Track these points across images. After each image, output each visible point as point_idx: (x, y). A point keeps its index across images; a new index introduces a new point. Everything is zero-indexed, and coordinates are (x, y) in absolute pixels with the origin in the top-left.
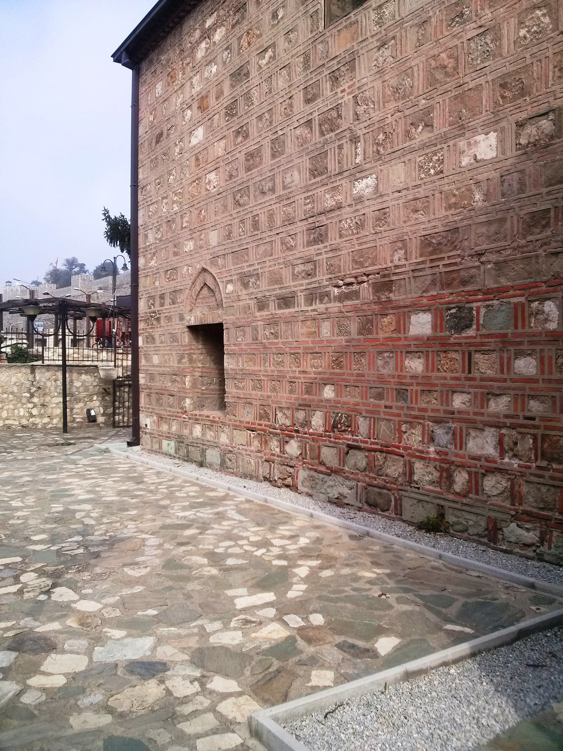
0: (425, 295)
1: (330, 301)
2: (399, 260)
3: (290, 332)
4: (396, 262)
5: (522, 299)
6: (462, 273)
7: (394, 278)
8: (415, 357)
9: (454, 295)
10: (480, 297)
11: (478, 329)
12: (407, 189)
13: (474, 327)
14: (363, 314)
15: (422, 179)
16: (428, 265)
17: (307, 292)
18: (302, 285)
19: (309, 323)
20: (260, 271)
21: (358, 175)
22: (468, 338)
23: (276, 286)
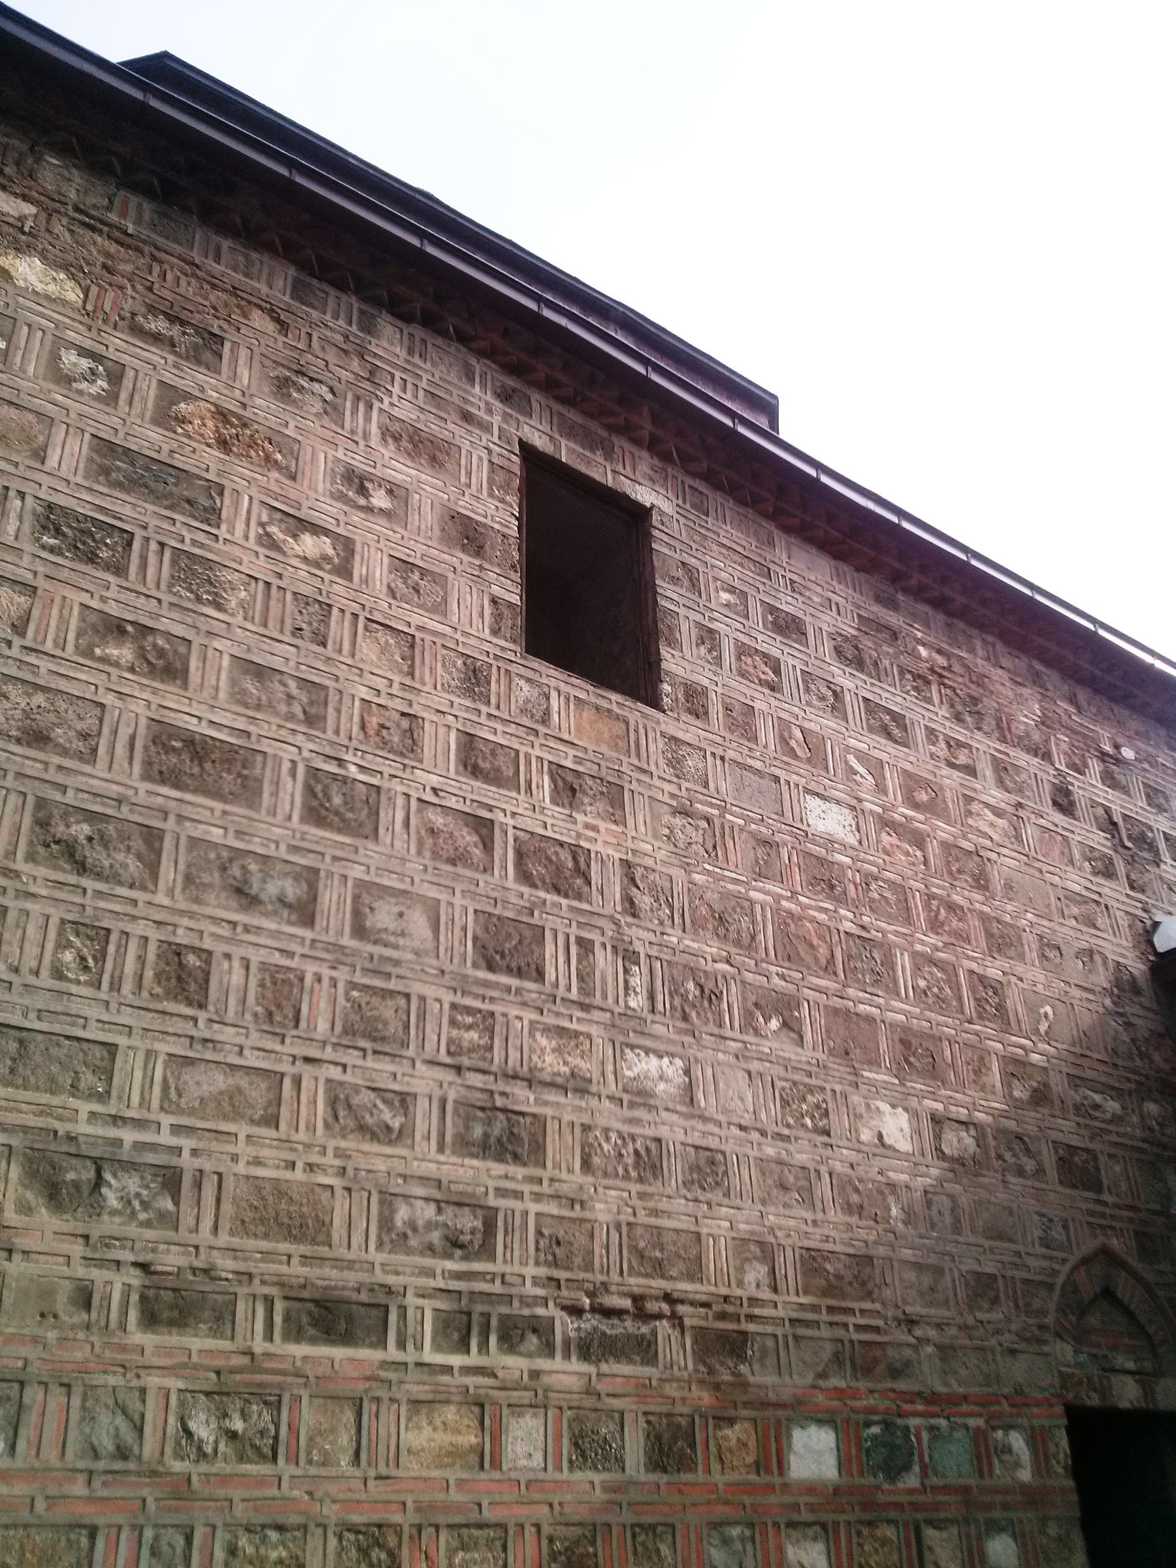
0: (821, 1383)
1: (548, 1349)
2: (758, 1286)
3: (345, 1439)
4: (752, 1291)
5: (980, 1422)
6: (891, 1352)
7: (752, 1327)
8: (805, 1537)
9: (876, 1395)
10: (920, 1407)
11: (924, 1475)
12: (763, 1133)
13: (917, 1468)
14: (664, 1409)
15: (788, 1126)
16: (824, 1317)
17: (442, 1304)
18: (430, 1273)
19: (450, 1413)
20: (186, 1161)
21: (633, 1038)
22: (911, 1491)
23: (284, 1247)
